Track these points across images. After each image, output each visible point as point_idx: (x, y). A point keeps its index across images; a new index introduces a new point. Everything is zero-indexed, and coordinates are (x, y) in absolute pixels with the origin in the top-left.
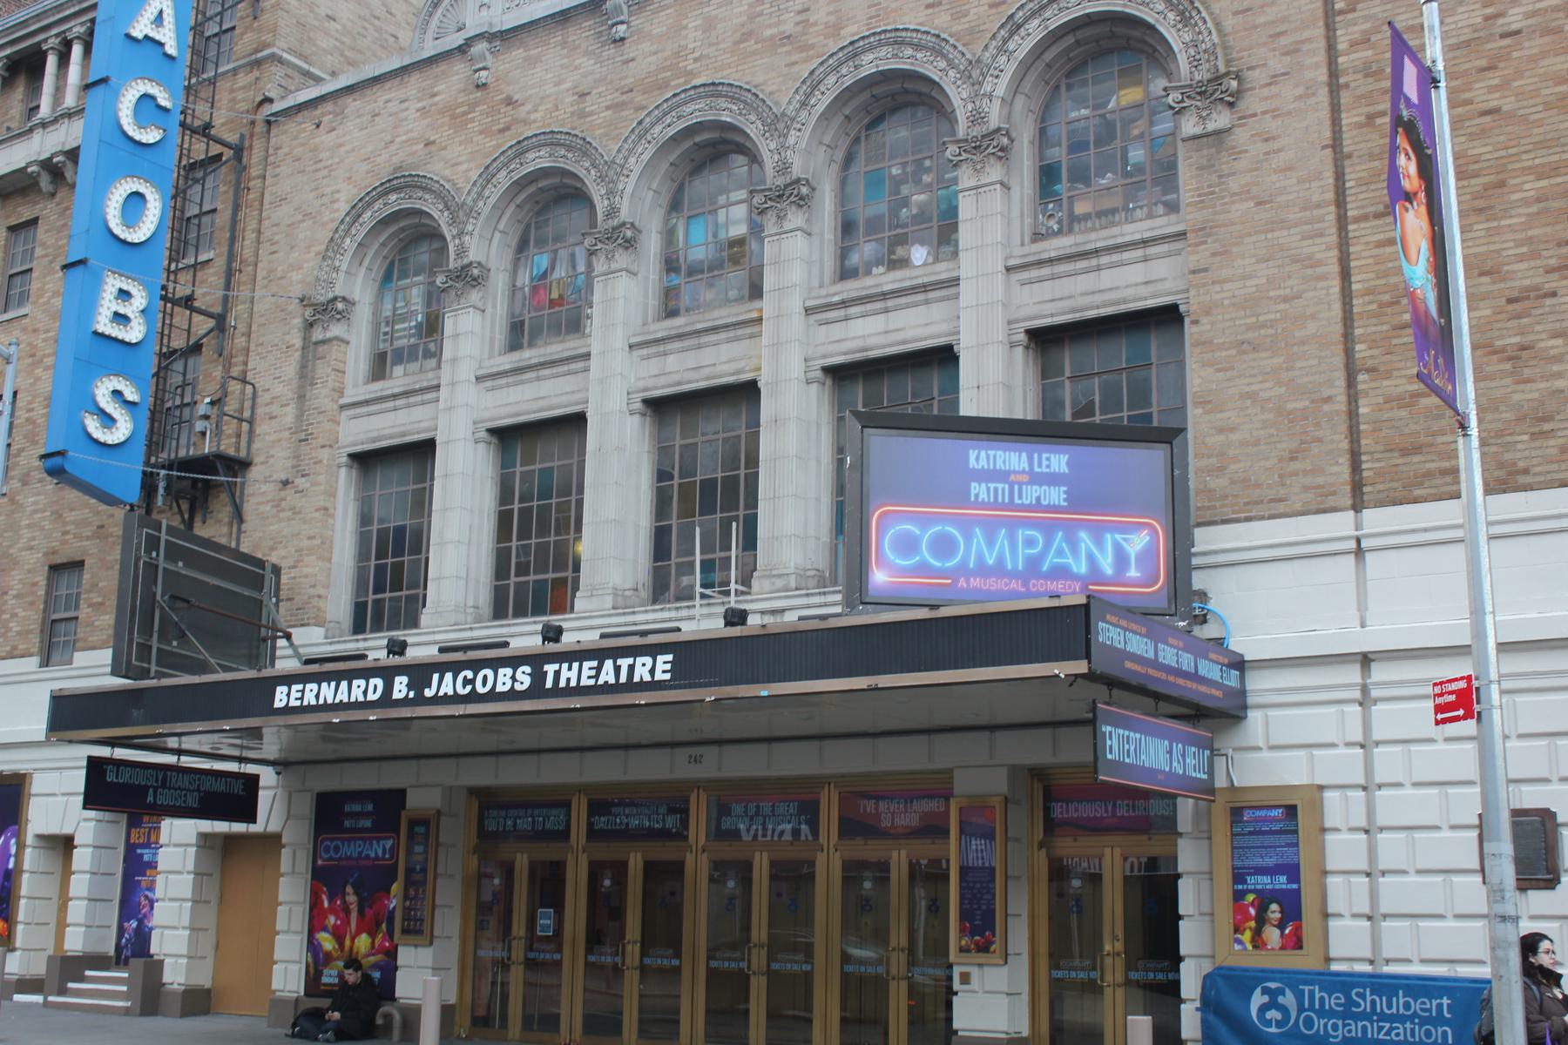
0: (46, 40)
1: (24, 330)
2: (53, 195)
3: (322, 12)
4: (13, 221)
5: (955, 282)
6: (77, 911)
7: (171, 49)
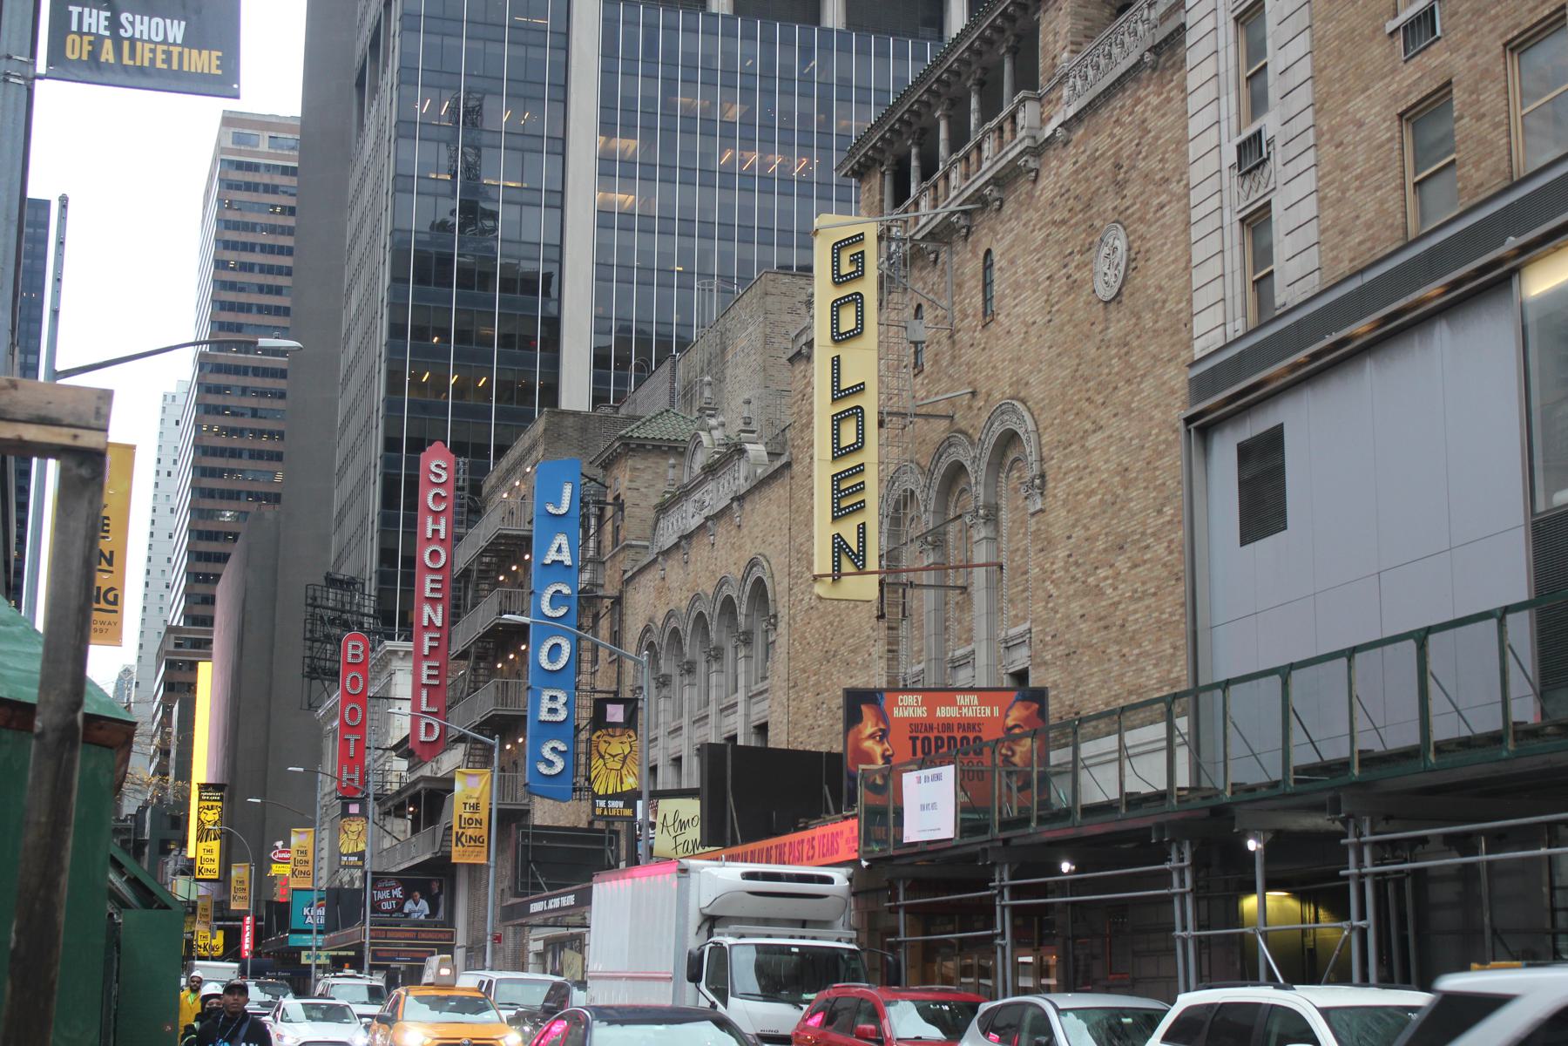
5: (735, 704)
7: (568, 562)
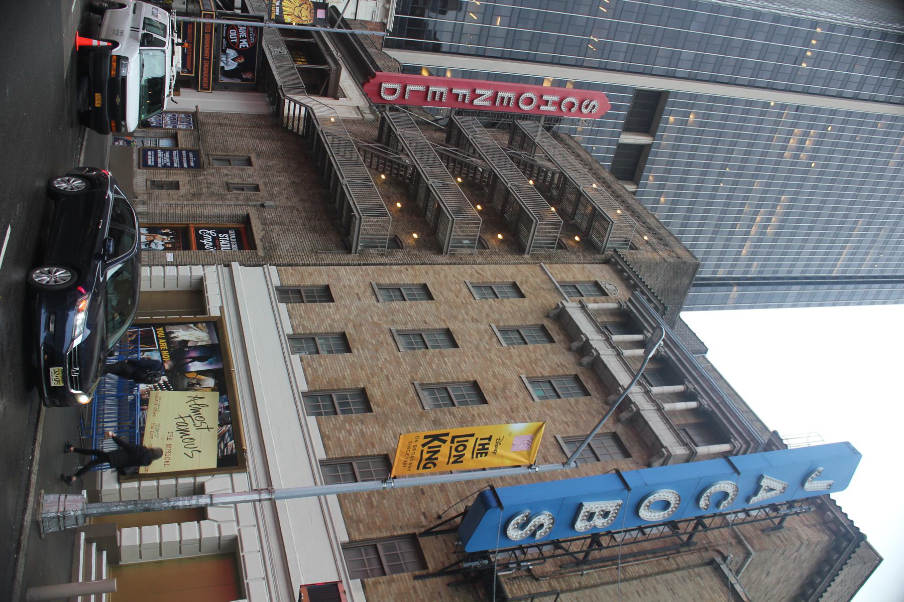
0: (690, 382)
1: (525, 401)
3: (772, 569)
4: (582, 378)
6: (151, 534)
7: (754, 500)
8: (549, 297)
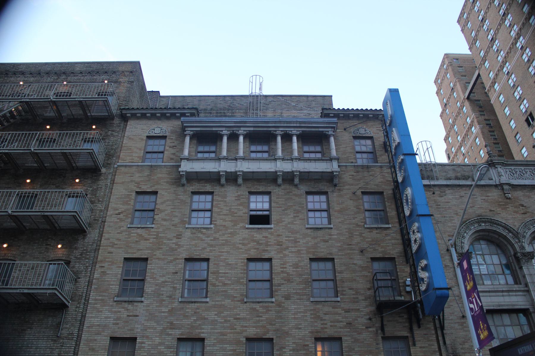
1: (271, 234)
2: (279, 186)
4: (253, 190)
8: (160, 175)
